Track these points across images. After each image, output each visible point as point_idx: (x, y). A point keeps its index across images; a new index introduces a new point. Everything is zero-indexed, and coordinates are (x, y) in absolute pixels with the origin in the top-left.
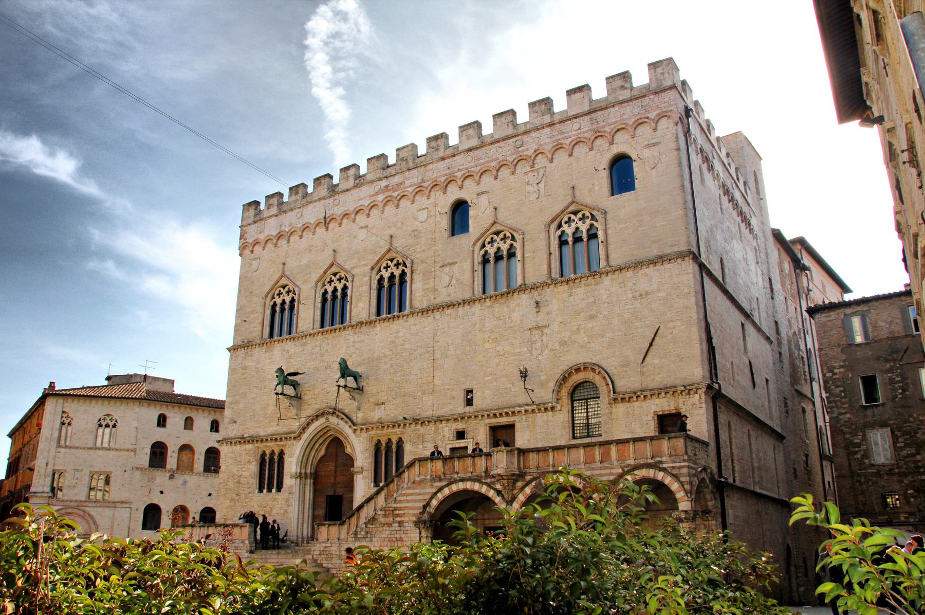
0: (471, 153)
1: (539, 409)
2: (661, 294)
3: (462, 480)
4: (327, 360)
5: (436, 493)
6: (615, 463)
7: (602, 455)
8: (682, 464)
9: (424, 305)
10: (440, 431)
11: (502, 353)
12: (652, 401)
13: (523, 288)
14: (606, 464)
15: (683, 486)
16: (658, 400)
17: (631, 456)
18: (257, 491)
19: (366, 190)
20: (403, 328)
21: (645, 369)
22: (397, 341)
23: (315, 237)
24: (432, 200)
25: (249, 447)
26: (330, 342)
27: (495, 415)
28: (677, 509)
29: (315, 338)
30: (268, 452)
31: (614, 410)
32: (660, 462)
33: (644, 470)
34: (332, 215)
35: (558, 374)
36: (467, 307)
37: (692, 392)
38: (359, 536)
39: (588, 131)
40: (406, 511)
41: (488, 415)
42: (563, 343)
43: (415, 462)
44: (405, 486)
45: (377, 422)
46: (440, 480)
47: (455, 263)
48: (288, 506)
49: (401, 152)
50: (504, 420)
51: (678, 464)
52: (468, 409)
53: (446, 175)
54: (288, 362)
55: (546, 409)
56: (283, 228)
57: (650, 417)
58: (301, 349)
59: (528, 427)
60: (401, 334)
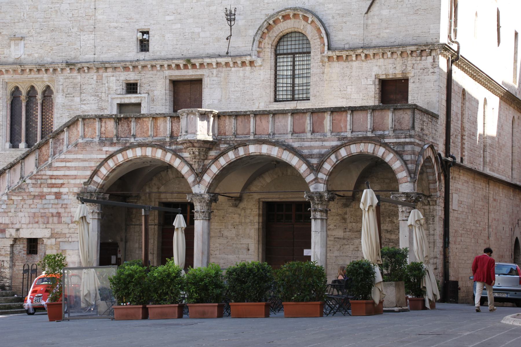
1: (235, 63)
3: (141, 145)
5: (106, 160)
6: (329, 134)
7: (313, 124)
8: (408, 140)
10: (105, 81)
12: (374, 61)
14: (318, 136)
15: (406, 164)
16: (382, 60)
17: (348, 127)
21: (369, 22)
27: (178, 66)
28: (398, 191)
31: (326, 70)
32: (383, 137)
33: (362, 144)
35: (260, 19)
37: (424, 54)
40: (65, 181)
41: (169, 66)
43: (78, 120)
44: (65, 149)
46: (112, 144)
50: (190, 73)
51: (402, 140)
52: (142, 56)
55: (243, 63)
57: (370, 81)
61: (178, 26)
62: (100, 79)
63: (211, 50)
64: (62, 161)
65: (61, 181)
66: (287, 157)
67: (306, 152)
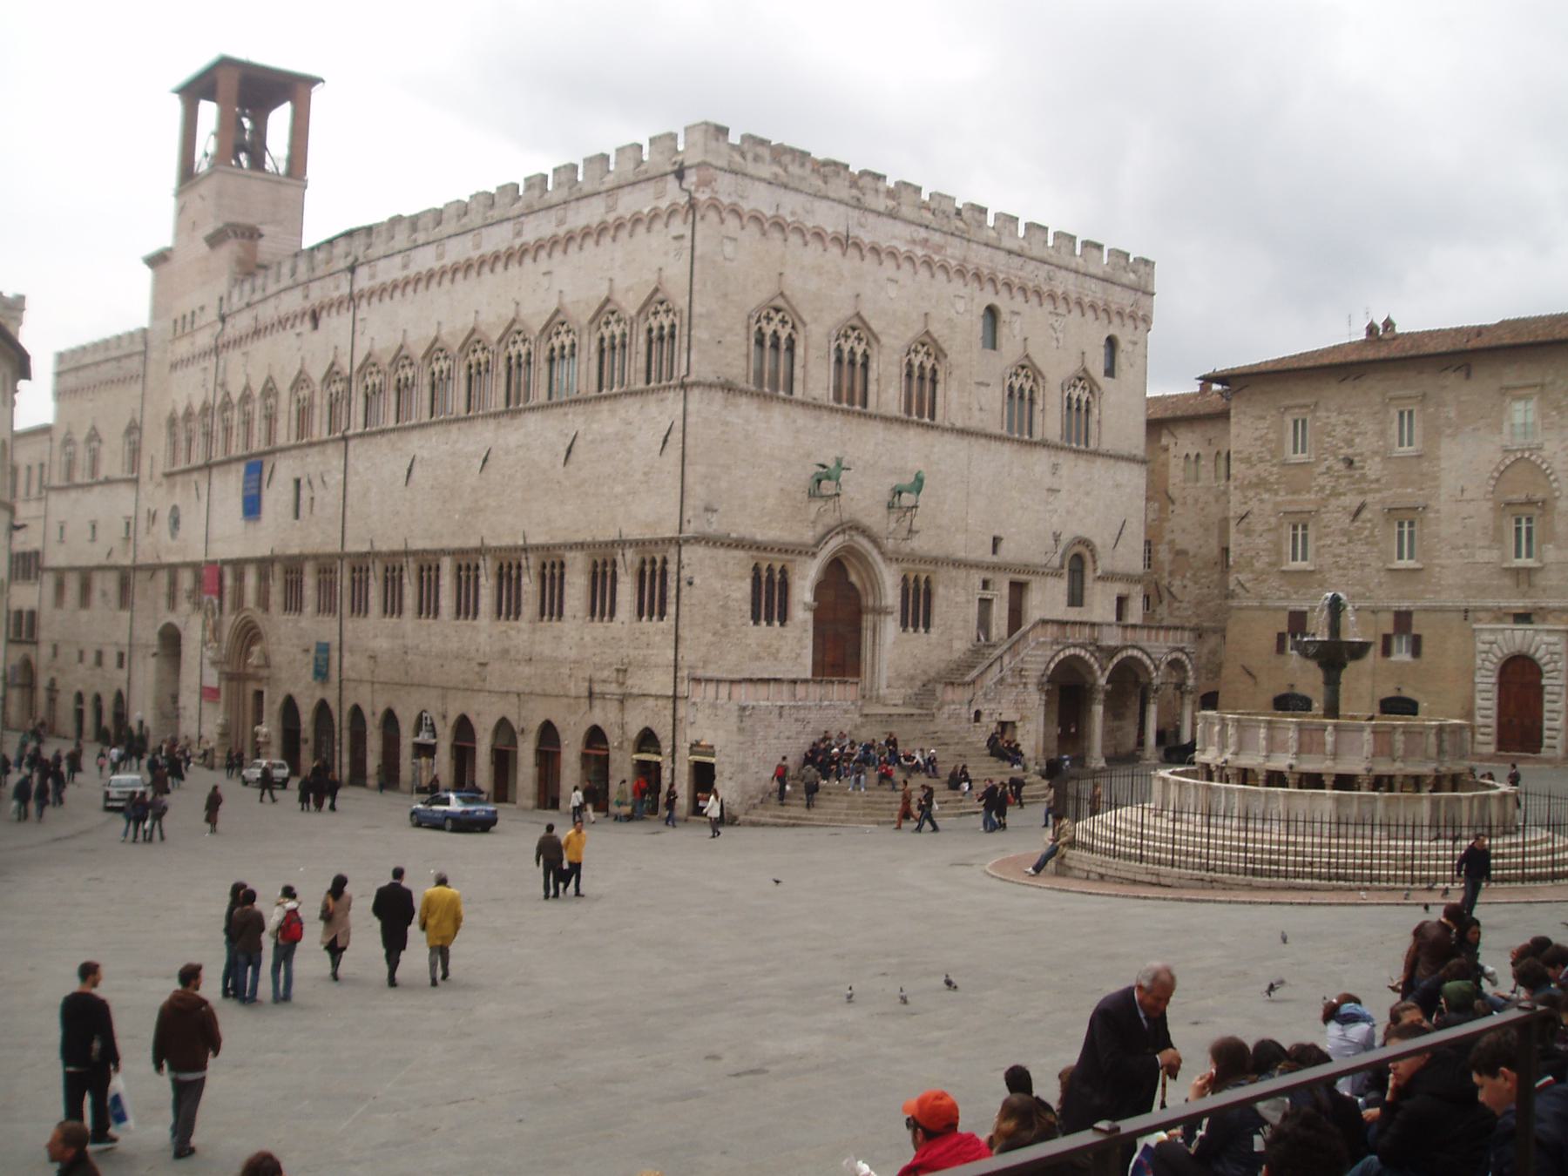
2: (1128, 490)
3: (1075, 646)
9: (959, 424)
13: (1044, 444)
18: (751, 623)
19: (899, 228)
25: (740, 554)
30: (764, 566)
36: (998, 443)
45: (907, 554)
46: (1058, 643)
47: (988, 385)
48: (802, 648)
50: (1022, 577)
56: (781, 212)
60: (936, 450)
62: (967, 576)
63: (1039, 559)
64: (1031, 656)
66: (1145, 658)
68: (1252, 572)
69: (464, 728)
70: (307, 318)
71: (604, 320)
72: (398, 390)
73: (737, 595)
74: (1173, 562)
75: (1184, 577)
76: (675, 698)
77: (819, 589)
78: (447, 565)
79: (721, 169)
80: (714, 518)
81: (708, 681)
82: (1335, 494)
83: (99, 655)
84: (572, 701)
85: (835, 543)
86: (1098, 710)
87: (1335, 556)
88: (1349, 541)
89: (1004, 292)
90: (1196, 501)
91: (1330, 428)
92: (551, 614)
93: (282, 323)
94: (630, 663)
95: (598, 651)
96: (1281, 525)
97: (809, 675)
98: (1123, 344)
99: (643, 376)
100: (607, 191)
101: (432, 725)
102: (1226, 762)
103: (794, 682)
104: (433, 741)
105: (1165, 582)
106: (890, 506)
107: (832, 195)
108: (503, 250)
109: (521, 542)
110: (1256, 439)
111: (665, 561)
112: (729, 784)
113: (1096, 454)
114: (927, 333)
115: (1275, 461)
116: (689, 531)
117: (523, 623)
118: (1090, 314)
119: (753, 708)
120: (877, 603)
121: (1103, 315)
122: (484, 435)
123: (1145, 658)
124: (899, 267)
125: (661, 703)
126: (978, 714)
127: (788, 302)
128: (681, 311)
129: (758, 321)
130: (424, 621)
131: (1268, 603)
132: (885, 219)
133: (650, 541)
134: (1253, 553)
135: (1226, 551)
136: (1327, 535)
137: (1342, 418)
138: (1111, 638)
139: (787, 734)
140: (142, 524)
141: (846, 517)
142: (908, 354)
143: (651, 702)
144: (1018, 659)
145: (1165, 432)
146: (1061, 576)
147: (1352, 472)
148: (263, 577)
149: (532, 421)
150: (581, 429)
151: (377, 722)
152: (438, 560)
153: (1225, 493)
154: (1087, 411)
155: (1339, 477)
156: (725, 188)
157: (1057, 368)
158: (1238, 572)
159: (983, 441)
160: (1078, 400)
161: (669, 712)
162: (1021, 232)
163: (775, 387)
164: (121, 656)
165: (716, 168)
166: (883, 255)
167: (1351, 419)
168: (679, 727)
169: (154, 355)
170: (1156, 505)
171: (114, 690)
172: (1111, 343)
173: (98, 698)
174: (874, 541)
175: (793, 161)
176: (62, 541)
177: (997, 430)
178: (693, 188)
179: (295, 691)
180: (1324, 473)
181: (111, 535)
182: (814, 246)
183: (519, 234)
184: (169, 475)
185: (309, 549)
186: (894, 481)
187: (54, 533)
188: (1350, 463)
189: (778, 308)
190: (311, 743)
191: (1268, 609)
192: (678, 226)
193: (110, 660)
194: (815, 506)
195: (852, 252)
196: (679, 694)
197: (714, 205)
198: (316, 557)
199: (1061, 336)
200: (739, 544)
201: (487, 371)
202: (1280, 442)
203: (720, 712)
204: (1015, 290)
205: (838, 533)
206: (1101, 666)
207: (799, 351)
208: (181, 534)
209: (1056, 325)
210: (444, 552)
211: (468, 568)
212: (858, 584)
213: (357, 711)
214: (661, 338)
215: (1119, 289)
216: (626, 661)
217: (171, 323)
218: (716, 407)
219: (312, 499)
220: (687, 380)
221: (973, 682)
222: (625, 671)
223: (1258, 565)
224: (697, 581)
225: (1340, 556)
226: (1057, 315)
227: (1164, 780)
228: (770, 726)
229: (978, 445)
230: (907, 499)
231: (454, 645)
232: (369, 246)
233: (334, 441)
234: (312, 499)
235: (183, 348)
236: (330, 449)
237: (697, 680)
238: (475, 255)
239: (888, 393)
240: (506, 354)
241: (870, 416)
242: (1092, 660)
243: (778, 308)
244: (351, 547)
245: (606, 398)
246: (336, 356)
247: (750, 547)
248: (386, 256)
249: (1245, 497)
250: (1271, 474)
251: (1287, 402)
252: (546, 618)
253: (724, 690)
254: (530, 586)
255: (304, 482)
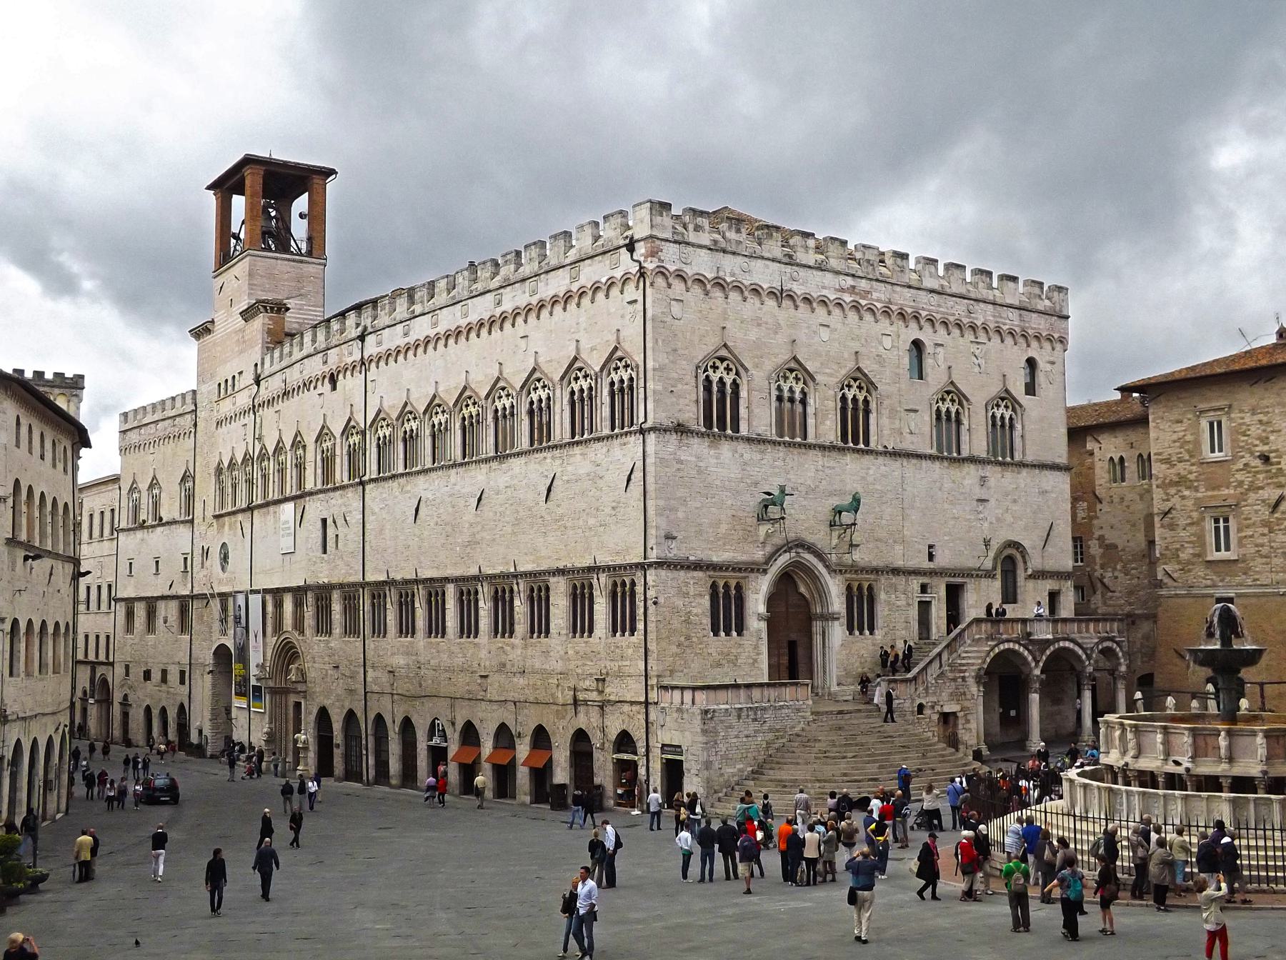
0: (933, 294)
2: (1054, 495)
3: (1008, 641)
4: (793, 480)
6: (1094, 634)
11: (957, 516)
13: (973, 460)
19: (829, 278)
20: (873, 465)
22: (868, 478)
23: (765, 308)
24: (894, 328)
25: (699, 574)
26: (796, 458)
27: (954, 576)
29: (777, 448)
30: (721, 583)
32: (1114, 636)
34: (790, 290)
36: (929, 462)
38: (930, 691)
39: (1017, 326)
42: (998, 520)
46: (993, 639)
48: (758, 654)
49: (867, 252)
50: (959, 580)
53: (912, 307)
54: (743, 470)
56: (721, 274)
57: (1047, 593)
58: (759, 457)
59: (975, 589)
60: (871, 472)
61: (951, 544)
62: (907, 581)
63: (972, 563)
64: (967, 652)
65: (965, 668)
66: (1077, 649)
67: (1085, 646)
68: (1179, 563)
69: (470, 734)
70: (327, 380)
71: (574, 376)
72: (405, 440)
73: (700, 611)
74: (1103, 556)
75: (1114, 569)
76: (647, 703)
77: (771, 601)
78: (451, 590)
79: (667, 240)
80: (674, 544)
81: (674, 688)
82: (1254, 488)
83: (164, 672)
84: (560, 708)
85: (784, 559)
86: (1035, 698)
87: (1257, 546)
88: (1270, 532)
89: (927, 326)
90: (1122, 499)
91: (1244, 428)
92: (540, 633)
93: (306, 385)
94: (607, 674)
95: (580, 663)
96: (1203, 519)
97: (765, 679)
98: (1042, 365)
99: (608, 423)
100: (571, 264)
101: (444, 730)
102: (1127, 764)
103: (749, 686)
104: (444, 745)
105: (1097, 574)
106: (831, 526)
107: (766, 255)
108: (487, 319)
109: (512, 570)
110: (1175, 442)
111: (633, 584)
112: (696, 779)
113: (1022, 465)
114: (859, 369)
115: (1193, 461)
116: (653, 556)
117: (516, 640)
118: (1009, 340)
119: (714, 711)
120: (825, 610)
121: (1021, 340)
122: (477, 477)
123: (1077, 649)
124: (829, 313)
125: (635, 708)
126: (921, 708)
127: (730, 352)
128: (637, 366)
129: (706, 370)
130: (433, 640)
131: (1195, 591)
132: (815, 272)
133: (620, 567)
134: (1178, 546)
135: (1151, 543)
136: (1248, 527)
137: (1256, 418)
138: (1043, 632)
139: (746, 733)
140: (197, 559)
141: (792, 536)
142: (842, 389)
143: (626, 708)
144: (954, 655)
145: (1089, 438)
146: (994, 577)
147: (1270, 468)
148: (298, 605)
149: (516, 464)
150: (559, 471)
151: (397, 729)
152: (444, 586)
153: (1149, 491)
154: (1012, 427)
155: (1257, 472)
156: (671, 256)
157: (979, 392)
158: (1167, 564)
159: (914, 461)
160: (1002, 418)
161: (642, 717)
162: (941, 272)
163: (722, 427)
164: (182, 673)
165: (662, 240)
166: (815, 305)
167: (1265, 419)
168: (652, 729)
169: (202, 414)
170: (1086, 504)
171: (178, 703)
172: (1031, 363)
173: (163, 711)
174: (819, 555)
175: (730, 228)
176: (130, 575)
177: (929, 451)
178: (642, 259)
179: (327, 703)
180: (1241, 470)
181: (172, 568)
182: (753, 301)
183: (499, 303)
184: (217, 517)
185: (335, 580)
186: (835, 501)
187: (124, 569)
188: (1265, 459)
189: (725, 357)
190: (342, 749)
191: (1195, 596)
192: (632, 292)
193: (173, 677)
194: (764, 529)
195: (787, 303)
196: (650, 701)
197: (661, 272)
198: (341, 586)
199: (982, 361)
200: (697, 566)
201: (478, 422)
202: (1197, 443)
203: (685, 716)
204: (937, 325)
205: (785, 552)
206: (1034, 658)
207: (743, 394)
208: (229, 567)
209: (977, 352)
210: (447, 580)
211: (469, 592)
212: (808, 596)
213: (379, 719)
214: (622, 390)
215: (1034, 315)
216: (604, 671)
217: (216, 386)
218: (671, 448)
219: (337, 535)
220: (645, 426)
221: (915, 678)
222: (604, 680)
223: (1184, 556)
224: (661, 600)
225: (1262, 545)
226: (978, 343)
227: (1071, 781)
228: (730, 727)
229: (910, 466)
230: (846, 518)
231: (459, 660)
232: (375, 318)
233: (351, 485)
234: (337, 535)
235: (226, 407)
236: (350, 493)
237: (665, 688)
238: (463, 323)
239: (825, 427)
240: (494, 408)
241: (810, 446)
242: (1026, 653)
243: (725, 357)
244: (370, 577)
245: (578, 443)
246: (352, 413)
247: (707, 568)
248: (389, 327)
249: (1167, 494)
250: (1191, 473)
251: (1202, 406)
252: (535, 635)
253: (688, 695)
254: (520, 607)
255: (329, 522)
